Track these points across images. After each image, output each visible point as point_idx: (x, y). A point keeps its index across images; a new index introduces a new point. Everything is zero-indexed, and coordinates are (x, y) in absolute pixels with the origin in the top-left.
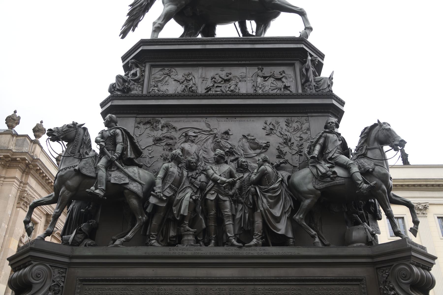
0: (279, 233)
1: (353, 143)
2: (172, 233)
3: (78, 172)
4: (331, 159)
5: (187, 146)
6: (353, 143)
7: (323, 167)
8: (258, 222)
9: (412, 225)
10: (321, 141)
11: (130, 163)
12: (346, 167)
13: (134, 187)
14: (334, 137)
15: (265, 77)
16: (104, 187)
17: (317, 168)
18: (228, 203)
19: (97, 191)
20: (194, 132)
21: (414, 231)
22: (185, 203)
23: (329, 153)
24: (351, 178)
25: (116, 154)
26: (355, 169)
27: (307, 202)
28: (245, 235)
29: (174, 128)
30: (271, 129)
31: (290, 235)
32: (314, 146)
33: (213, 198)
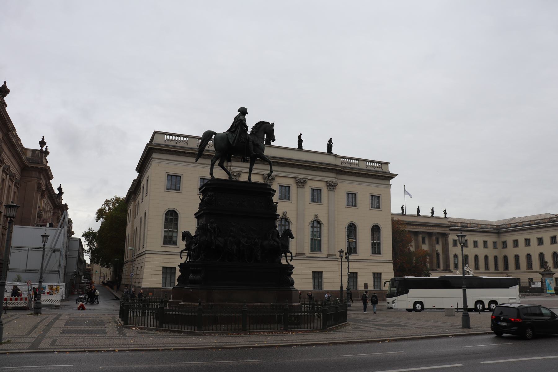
12: (277, 242)
26: (280, 245)
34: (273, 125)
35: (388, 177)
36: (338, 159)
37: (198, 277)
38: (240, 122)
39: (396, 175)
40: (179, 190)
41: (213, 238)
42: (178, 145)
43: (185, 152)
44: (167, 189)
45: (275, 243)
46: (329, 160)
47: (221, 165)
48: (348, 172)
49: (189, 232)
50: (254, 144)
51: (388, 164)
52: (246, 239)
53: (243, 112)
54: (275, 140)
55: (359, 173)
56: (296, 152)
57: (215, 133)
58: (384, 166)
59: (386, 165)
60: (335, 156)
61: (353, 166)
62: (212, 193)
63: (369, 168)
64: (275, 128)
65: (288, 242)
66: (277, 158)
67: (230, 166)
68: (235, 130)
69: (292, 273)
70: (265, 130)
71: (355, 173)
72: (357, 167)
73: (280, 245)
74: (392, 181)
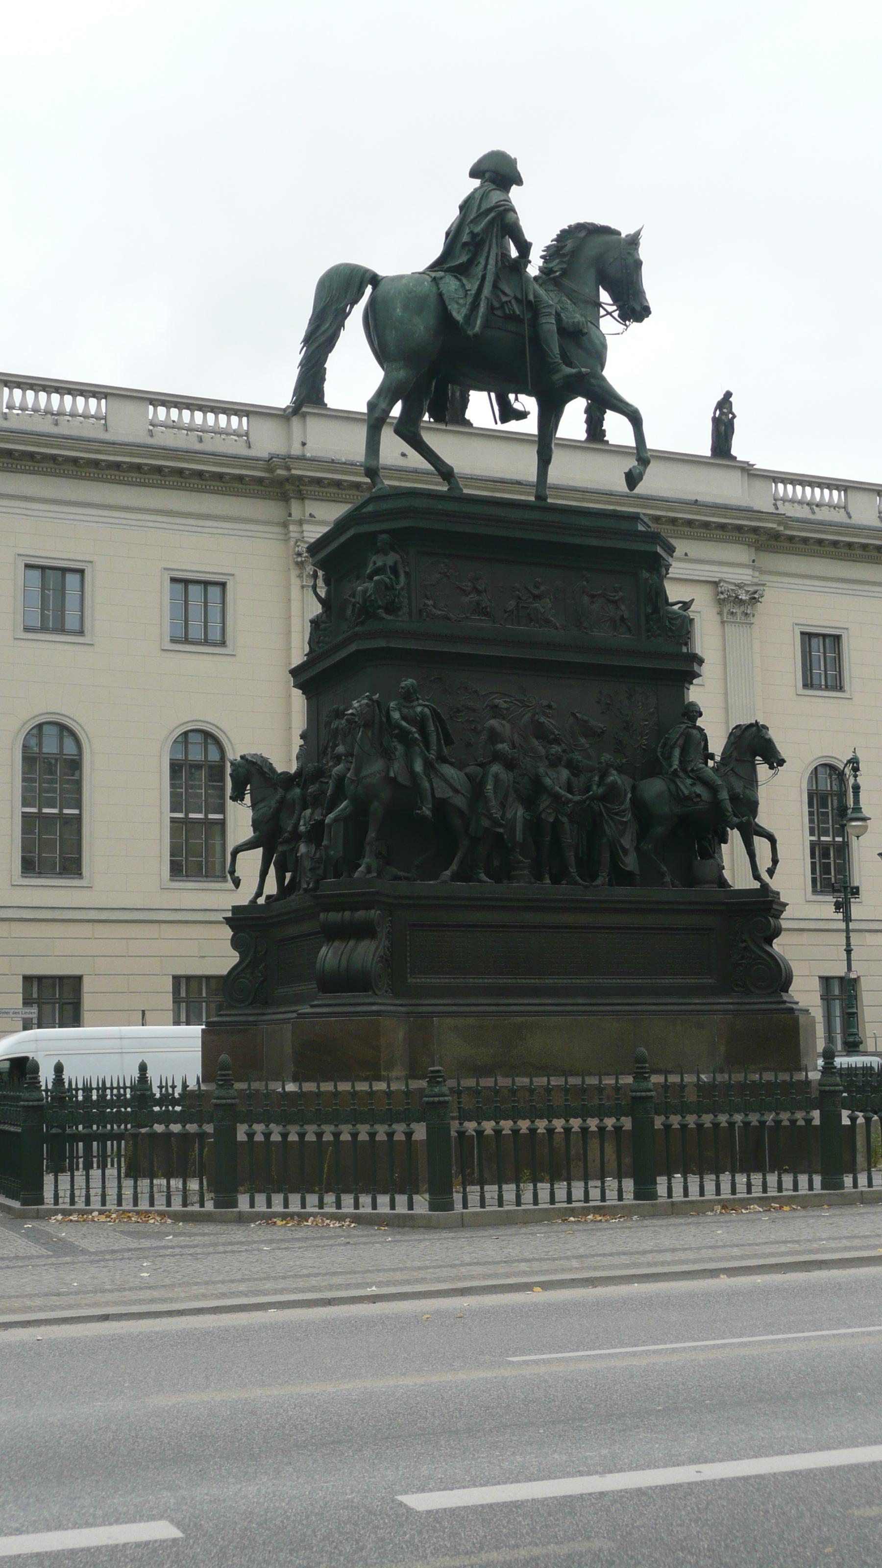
0: (627, 869)
1: (717, 745)
2: (496, 863)
3: (393, 781)
4: (692, 770)
5: (493, 722)
6: (717, 745)
7: (686, 786)
8: (606, 856)
9: (770, 864)
10: (681, 742)
11: (443, 760)
13: (460, 801)
14: (695, 732)
15: (593, 596)
16: (430, 806)
17: (677, 786)
18: (567, 826)
19: (428, 813)
20: (505, 702)
21: (771, 872)
22: (519, 827)
23: (691, 761)
24: (717, 803)
25: (432, 752)
26: (724, 795)
27: (660, 830)
28: (589, 872)
29: (476, 692)
30: (609, 704)
31: (637, 872)
32: (672, 747)
33: (551, 820)
34: (634, 241)
36: (759, 484)
38: (485, 224)
40: (81, 633)
41: (418, 767)
42: (63, 429)
43: (96, 463)
44: (27, 629)
45: (699, 789)
46: (721, 489)
47: (408, 431)
48: (805, 540)
49: (265, 760)
50: (563, 331)
52: (565, 773)
53: (497, 173)
55: (850, 545)
56: (579, 456)
57: (375, 280)
60: (747, 470)
61: (823, 515)
62: (391, 558)
64: (643, 253)
65: (752, 781)
66: (503, 481)
67: (300, 523)
68: (471, 262)
69: (777, 932)
70: (604, 264)
71: (835, 543)
72: (839, 517)
73: (724, 795)
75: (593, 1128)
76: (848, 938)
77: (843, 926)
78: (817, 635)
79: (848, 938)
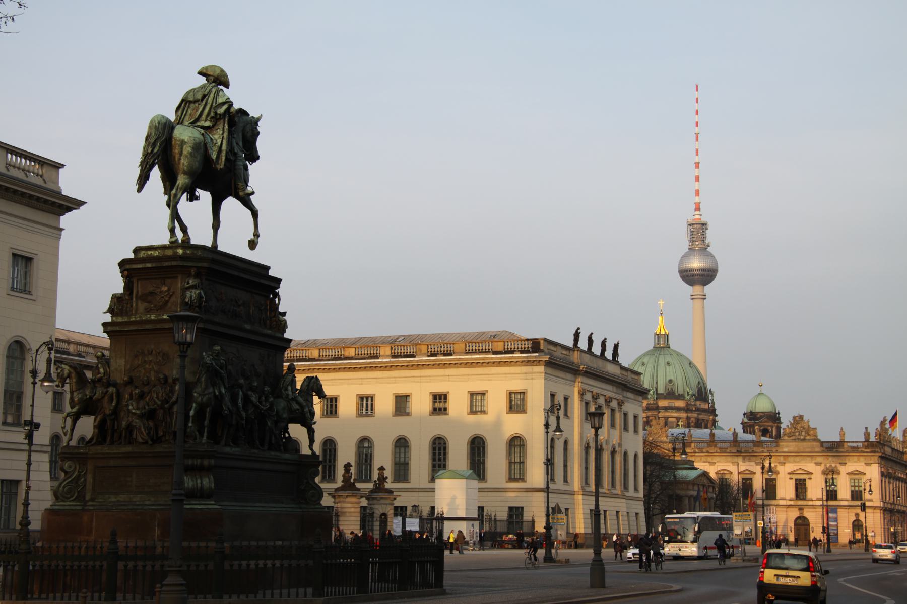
34: (256, 122)
35: (61, 206)
37: (207, 482)
39: (84, 203)
51: (58, 166)
54: (258, 158)
58: (46, 171)
59: (53, 171)
63: (14, 173)
68: (213, 126)
74: (66, 220)
75: (286, 565)
76: (30, 456)
77: (27, 448)
78: (23, 257)
79: (30, 456)
